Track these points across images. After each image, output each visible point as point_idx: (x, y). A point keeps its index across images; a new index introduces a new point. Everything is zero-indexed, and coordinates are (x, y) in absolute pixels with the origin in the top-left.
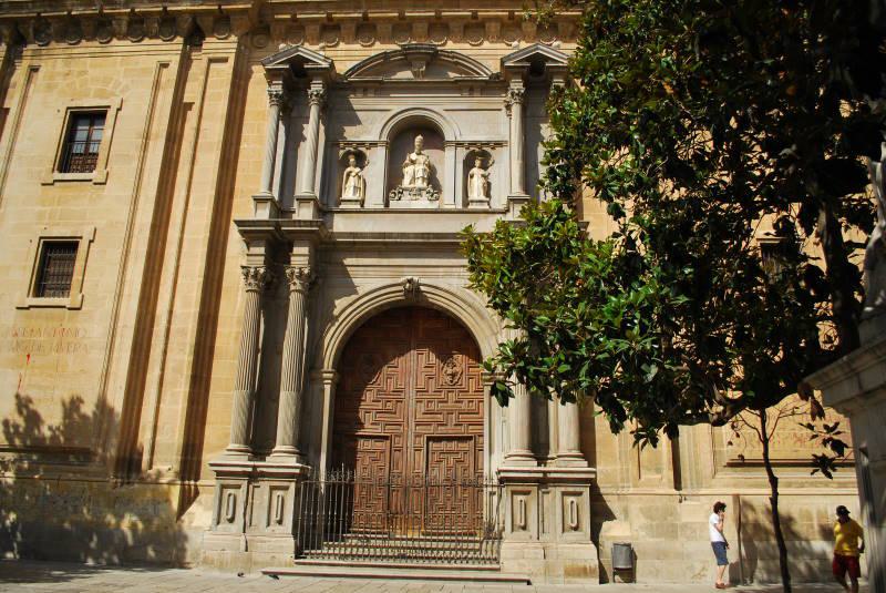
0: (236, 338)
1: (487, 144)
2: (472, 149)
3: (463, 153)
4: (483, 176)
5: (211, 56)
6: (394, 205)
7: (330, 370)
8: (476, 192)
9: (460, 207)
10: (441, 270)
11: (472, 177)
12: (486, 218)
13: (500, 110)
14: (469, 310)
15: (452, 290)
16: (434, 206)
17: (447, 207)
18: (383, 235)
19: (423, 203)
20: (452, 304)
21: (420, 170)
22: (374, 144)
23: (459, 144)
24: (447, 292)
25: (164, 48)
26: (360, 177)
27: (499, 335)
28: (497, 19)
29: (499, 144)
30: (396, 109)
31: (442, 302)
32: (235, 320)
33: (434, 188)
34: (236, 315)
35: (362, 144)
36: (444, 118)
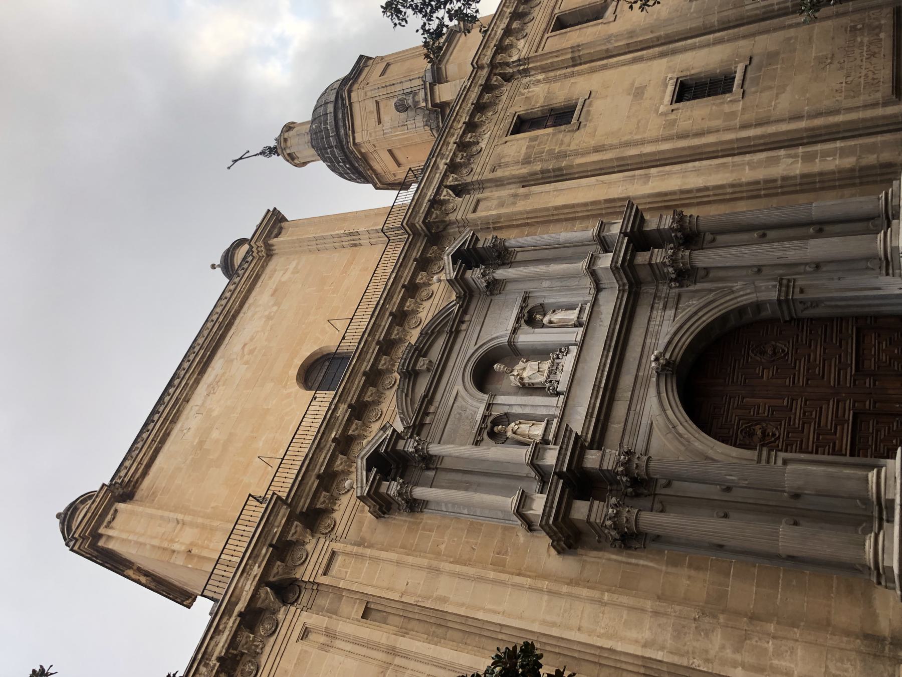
0: (698, 568)
1: (522, 308)
2: (523, 321)
3: (525, 327)
4: (554, 311)
5: (320, 572)
6: (562, 387)
7: (756, 453)
8: (573, 315)
9: (581, 330)
10: (648, 341)
11: (551, 322)
12: (599, 306)
13: (491, 300)
14: (700, 314)
15: (672, 331)
16: (574, 350)
17: (579, 339)
18: (596, 387)
19: (568, 362)
20: (691, 330)
21: (534, 365)
22: (489, 406)
23: (515, 331)
24: (675, 334)
25: (283, 632)
26: (520, 423)
27: (734, 289)
28: (403, 300)
29: (525, 300)
30: (459, 387)
31: (687, 340)
32: (671, 569)
33: (553, 351)
34: (664, 568)
35: (484, 418)
36: (484, 344)
